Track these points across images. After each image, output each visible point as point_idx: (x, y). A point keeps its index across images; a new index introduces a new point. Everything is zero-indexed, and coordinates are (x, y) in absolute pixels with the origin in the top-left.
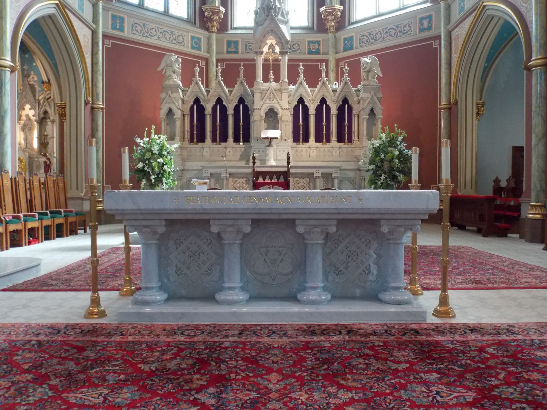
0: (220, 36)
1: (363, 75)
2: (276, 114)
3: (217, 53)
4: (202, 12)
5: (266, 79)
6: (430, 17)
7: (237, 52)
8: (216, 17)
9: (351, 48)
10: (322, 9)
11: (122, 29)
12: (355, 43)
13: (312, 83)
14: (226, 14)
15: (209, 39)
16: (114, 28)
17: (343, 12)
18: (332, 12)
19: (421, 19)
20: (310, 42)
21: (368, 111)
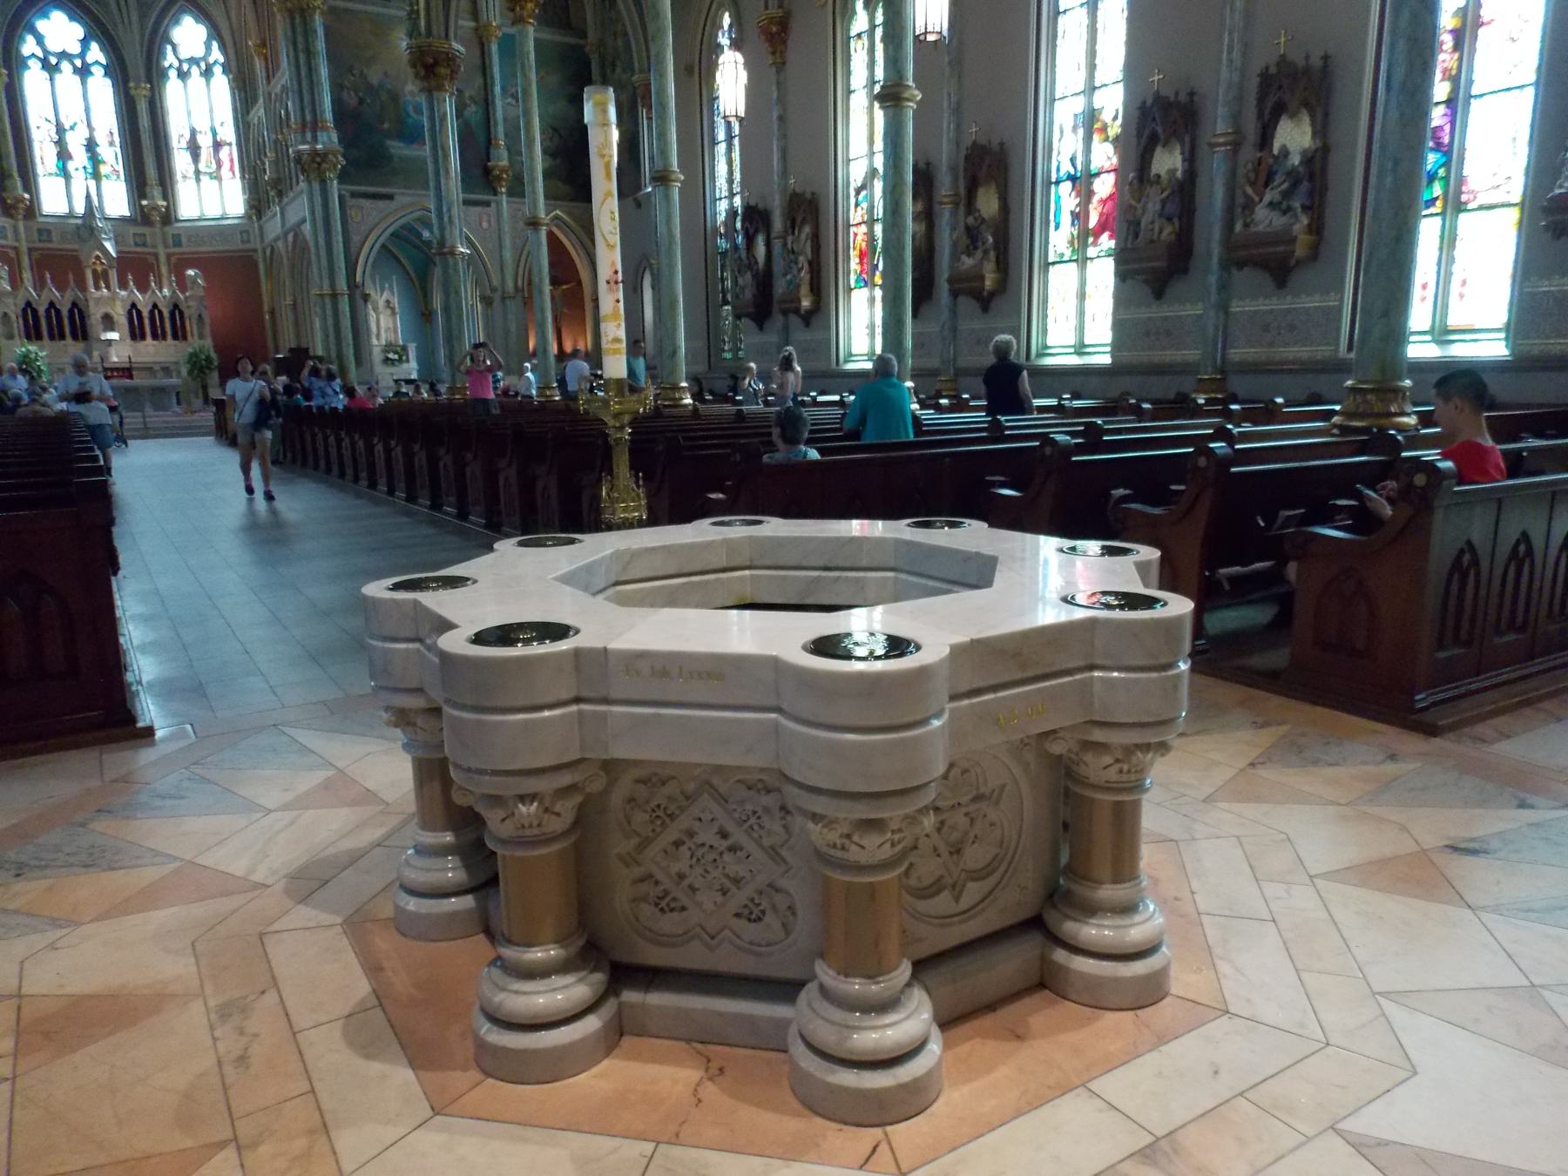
0: (30, 223)
3: (27, 241)
7: (50, 241)
8: (21, 205)
10: (144, 203)
12: (184, 240)
14: (31, 201)
17: (167, 208)
18: (156, 208)
19: (241, 233)
20: (134, 235)
21: (196, 316)
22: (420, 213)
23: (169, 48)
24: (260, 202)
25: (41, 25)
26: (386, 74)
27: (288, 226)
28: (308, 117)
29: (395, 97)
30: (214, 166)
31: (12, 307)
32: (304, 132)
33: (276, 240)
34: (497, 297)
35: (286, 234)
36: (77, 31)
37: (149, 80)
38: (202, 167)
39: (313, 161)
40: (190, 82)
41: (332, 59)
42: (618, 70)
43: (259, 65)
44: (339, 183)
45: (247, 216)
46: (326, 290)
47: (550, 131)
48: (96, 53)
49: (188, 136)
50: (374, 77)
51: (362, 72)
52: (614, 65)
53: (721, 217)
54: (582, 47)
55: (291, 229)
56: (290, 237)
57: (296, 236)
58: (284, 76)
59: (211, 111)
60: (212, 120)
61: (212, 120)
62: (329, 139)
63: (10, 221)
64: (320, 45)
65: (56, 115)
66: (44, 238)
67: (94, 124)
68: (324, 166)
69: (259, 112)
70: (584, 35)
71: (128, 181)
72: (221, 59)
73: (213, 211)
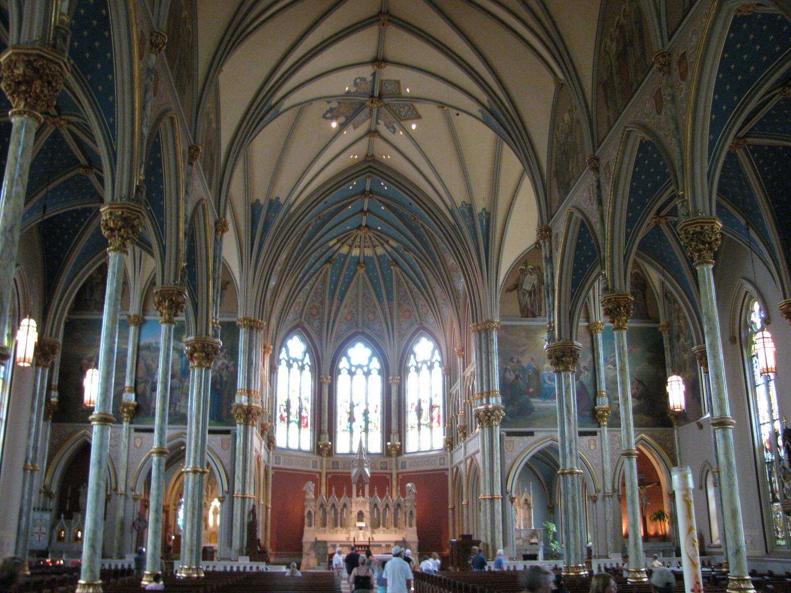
1: (407, 493)
2: (363, 514)
3: (327, 469)
4: (318, 446)
5: (358, 496)
6: (444, 458)
7: (338, 468)
9: (405, 468)
10: (389, 444)
11: (279, 464)
12: (407, 465)
13: (382, 495)
15: (322, 460)
16: (276, 463)
17: (401, 446)
18: (394, 446)
22: (549, 443)
23: (412, 356)
24: (452, 439)
25: (351, 352)
26: (532, 359)
27: (468, 454)
28: (485, 390)
29: (537, 373)
30: (429, 420)
31: (313, 507)
32: (482, 399)
33: (460, 463)
34: (600, 495)
35: (466, 460)
36: (368, 352)
37: (400, 375)
38: (422, 421)
39: (486, 415)
40: (421, 373)
41: (500, 354)
42: (682, 340)
43: (459, 361)
44: (501, 427)
45: (445, 449)
46: (488, 496)
47: (636, 382)
48: (376, 364)
49: (416, 404)
50: (525, 362)
51: (518, 361)
52: (678, 337)
53: (766, 437)
54: (655, 329)
55: (470, 456)
56: (469, 461)
57: (472, 460)
58: (472, 368)
59: (431, 389)
60: (431, 394)
61: (431, 394)
62: (496, 401)
63: (320, 458)
64: (495, 347)
65: (351, 398)
66: (336, 467)
67: (369, 402)
68: (492, 417)
69: (457, 387)
70: (657, 321)
71: (382, 432)
72: (439, 359)
73: (425, 447)
